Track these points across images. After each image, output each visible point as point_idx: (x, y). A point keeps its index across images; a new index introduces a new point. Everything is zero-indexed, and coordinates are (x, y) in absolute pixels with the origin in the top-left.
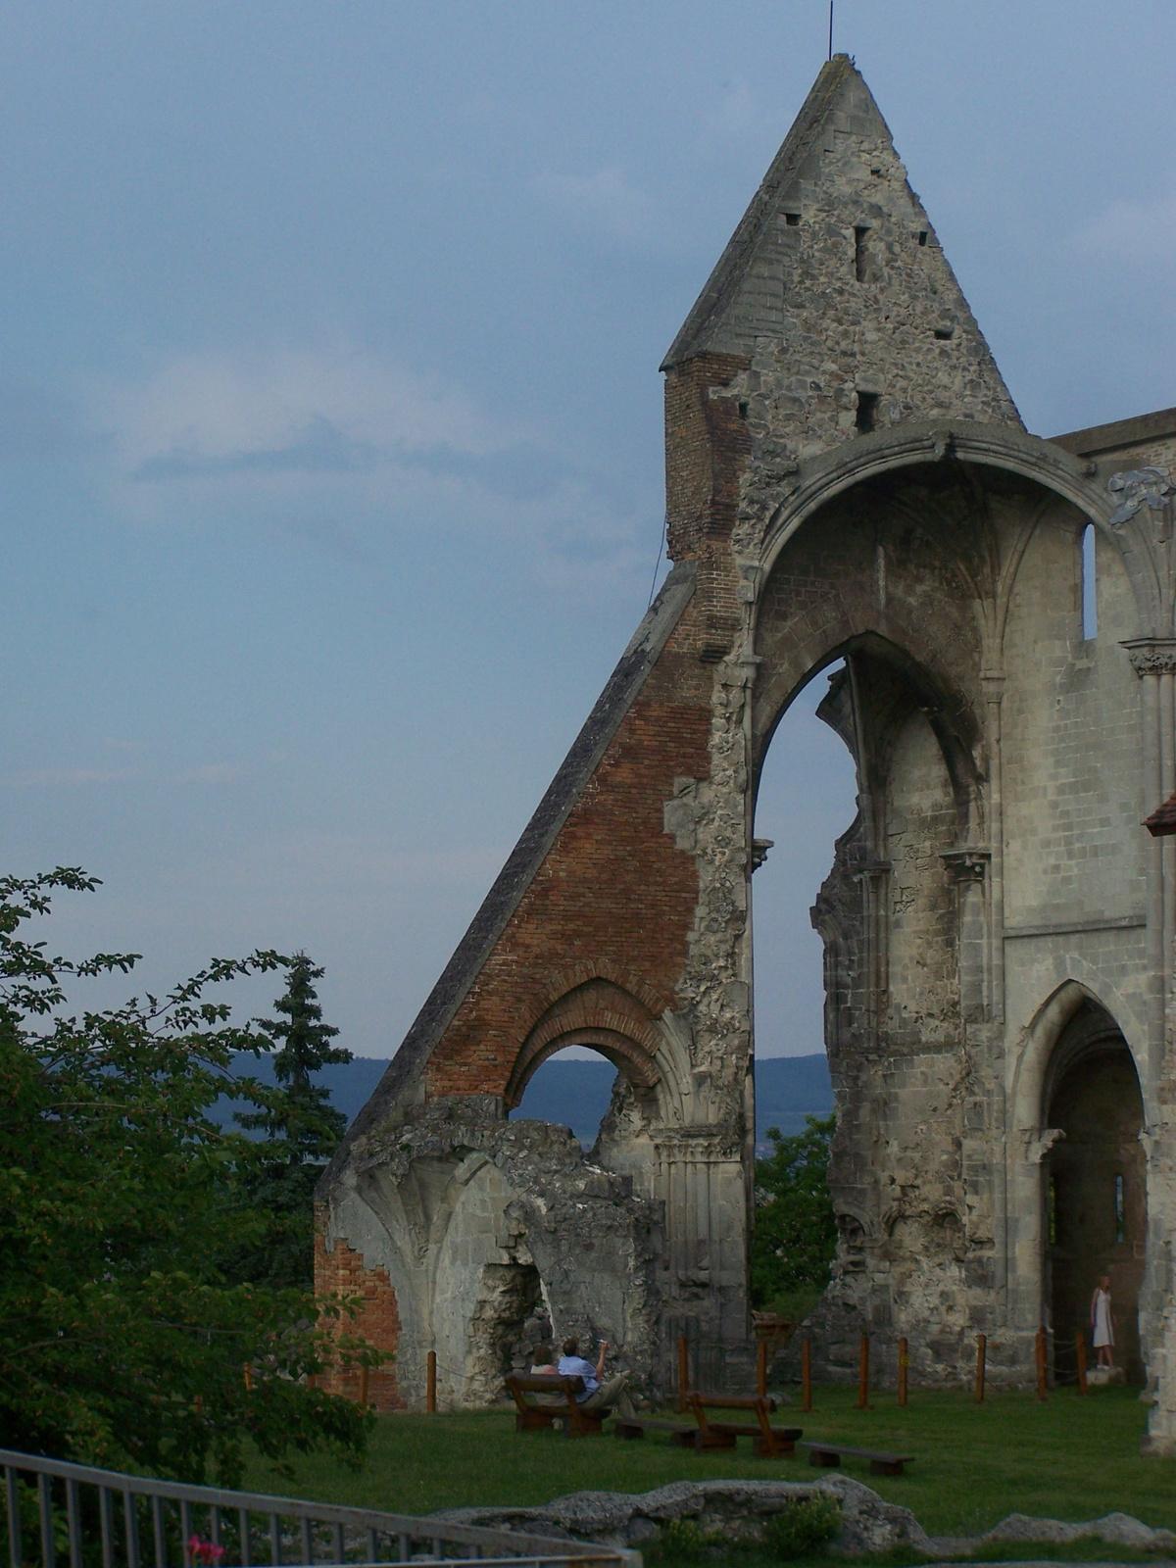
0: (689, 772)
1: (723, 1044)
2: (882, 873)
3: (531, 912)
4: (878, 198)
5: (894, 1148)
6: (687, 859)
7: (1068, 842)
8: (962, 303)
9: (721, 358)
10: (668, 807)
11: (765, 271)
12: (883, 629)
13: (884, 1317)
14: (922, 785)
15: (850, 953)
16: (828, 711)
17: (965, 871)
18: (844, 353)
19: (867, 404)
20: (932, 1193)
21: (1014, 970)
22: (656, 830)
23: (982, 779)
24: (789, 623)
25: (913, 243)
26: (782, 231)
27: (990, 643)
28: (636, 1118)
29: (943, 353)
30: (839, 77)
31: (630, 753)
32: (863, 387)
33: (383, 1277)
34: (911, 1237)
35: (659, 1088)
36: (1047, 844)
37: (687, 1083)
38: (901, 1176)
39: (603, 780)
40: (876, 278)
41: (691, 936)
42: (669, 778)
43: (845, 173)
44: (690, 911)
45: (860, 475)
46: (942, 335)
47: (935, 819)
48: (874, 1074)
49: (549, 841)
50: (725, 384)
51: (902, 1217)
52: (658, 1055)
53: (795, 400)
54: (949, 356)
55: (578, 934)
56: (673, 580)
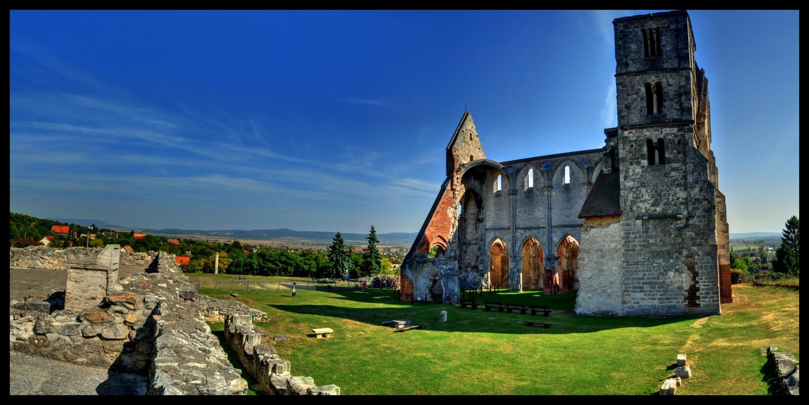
0: (450, 206)
2: (466, 220)
5: (467, 257)
6: (450, 219)
7: (497, 217)
9: (455, 148)
10: (448, 211)
12: (472, 187)
13: (465, 280)
14: (472, 209)
17: (480, 221)
19: (472, 157)
20: (473, 264)
21: (487, 234)
22: (446, 214)
23: (483, 208)
27: (484, 190)
31: (443, 203)
34: (469, 269)
36: (493, 217)
38: (468, 261)
39: (440, 207)
46: (480, 149)
48: (464, 247)
51: (468, 267)
55: (437, 229)
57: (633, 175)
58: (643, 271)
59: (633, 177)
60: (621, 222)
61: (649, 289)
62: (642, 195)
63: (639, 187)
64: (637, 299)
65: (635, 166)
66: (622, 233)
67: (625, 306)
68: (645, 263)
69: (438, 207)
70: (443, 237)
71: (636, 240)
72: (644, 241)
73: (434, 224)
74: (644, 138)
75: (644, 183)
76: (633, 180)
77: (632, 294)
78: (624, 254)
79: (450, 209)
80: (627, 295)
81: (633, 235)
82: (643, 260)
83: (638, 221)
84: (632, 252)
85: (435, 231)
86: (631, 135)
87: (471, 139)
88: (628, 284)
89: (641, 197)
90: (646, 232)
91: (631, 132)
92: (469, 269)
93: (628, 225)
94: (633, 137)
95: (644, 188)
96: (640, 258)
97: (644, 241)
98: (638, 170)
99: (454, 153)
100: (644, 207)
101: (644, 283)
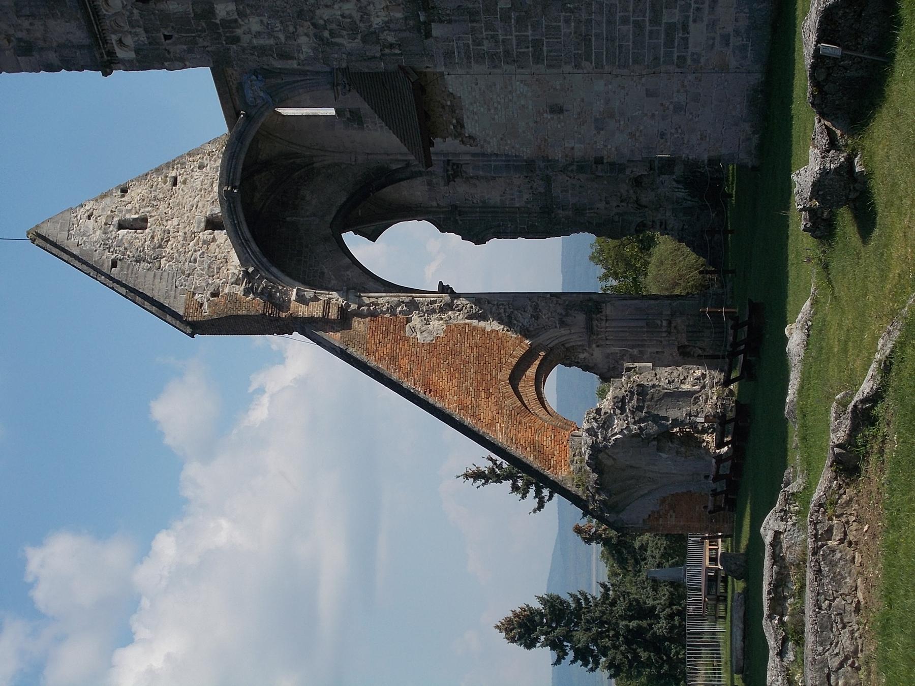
0: (403, 328)
1: (544, 311)
2: (454, 208)
3: (474, 416)
4: (103, 220)
6: (449, 331)
8: (158, 170)
10: (421, 341)
11: (141, 280)
12: (329, 218)
14: (414, 190)
15: (499, 226)
16: (373, 237)
18: (185, 239)
19: (212, 224)
24: (326, 271)
25: (127, 198)
26: (122, 269)
28: (582, 356)
29: (184, 182)
30: (39, 238)
31: (393, 359)
32: (203, 225)
33: (663, 501)
35: (567, 345)
37: (563, 331)
39: (407, 375)
40: (144, 220)
41: (488, 329)
42: (407, 339)
43: (89, 233)
44: (475, 328)
45: (248, 235)
47: (430, 183)
49: (439, 405)
50: (202, 304)
52: (550, 346)
53: (209, 267)
54: (186, 179)
55: (487, 390)
56: (303, 333)
57: (270, 35)
58: (609, 22)
59: (282, 37)
60: (441, 69)
61: (677, 11)
62: (343, 16)
63: (314, 25)
64: (714, 39)
65: (239, 32)
66: (475, 68)
67: (733, 63)
68: (584, 16)
69: (408, 384)
70: (514, 361)
71: (501, 38)
72: (506, 18)
73: (467, 402)
74: (135, 11)
75: (300, 14)
76: (293, 36)
77: (690, 45)
78: (550, 66)
79: (413, 330)
80: (696, 61)
81: (486, 42)
82: (573, 24)
83: (434, 33)
84: (545, 49)
85: (493, 399)
86: (129, 40)
87: (140, 224)
88: (655, 59)
89: (349, 20)
90: (473, 15)
91: (120, 42)
92: (646, 197)
93: (449, 55)
94: (136, 34)
95: (318, 12)
96: (564, 30)
97: (506, 18)
98: (254, 23)
99: (206, 310)
100: (383, 13)
101: (655, 21)
